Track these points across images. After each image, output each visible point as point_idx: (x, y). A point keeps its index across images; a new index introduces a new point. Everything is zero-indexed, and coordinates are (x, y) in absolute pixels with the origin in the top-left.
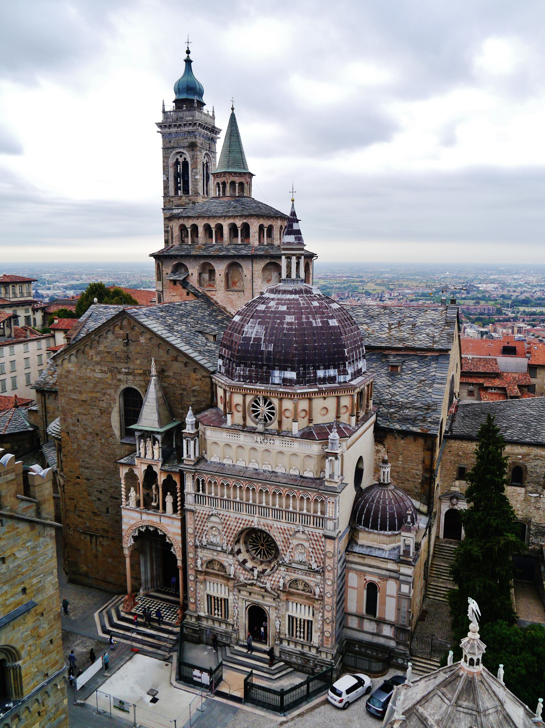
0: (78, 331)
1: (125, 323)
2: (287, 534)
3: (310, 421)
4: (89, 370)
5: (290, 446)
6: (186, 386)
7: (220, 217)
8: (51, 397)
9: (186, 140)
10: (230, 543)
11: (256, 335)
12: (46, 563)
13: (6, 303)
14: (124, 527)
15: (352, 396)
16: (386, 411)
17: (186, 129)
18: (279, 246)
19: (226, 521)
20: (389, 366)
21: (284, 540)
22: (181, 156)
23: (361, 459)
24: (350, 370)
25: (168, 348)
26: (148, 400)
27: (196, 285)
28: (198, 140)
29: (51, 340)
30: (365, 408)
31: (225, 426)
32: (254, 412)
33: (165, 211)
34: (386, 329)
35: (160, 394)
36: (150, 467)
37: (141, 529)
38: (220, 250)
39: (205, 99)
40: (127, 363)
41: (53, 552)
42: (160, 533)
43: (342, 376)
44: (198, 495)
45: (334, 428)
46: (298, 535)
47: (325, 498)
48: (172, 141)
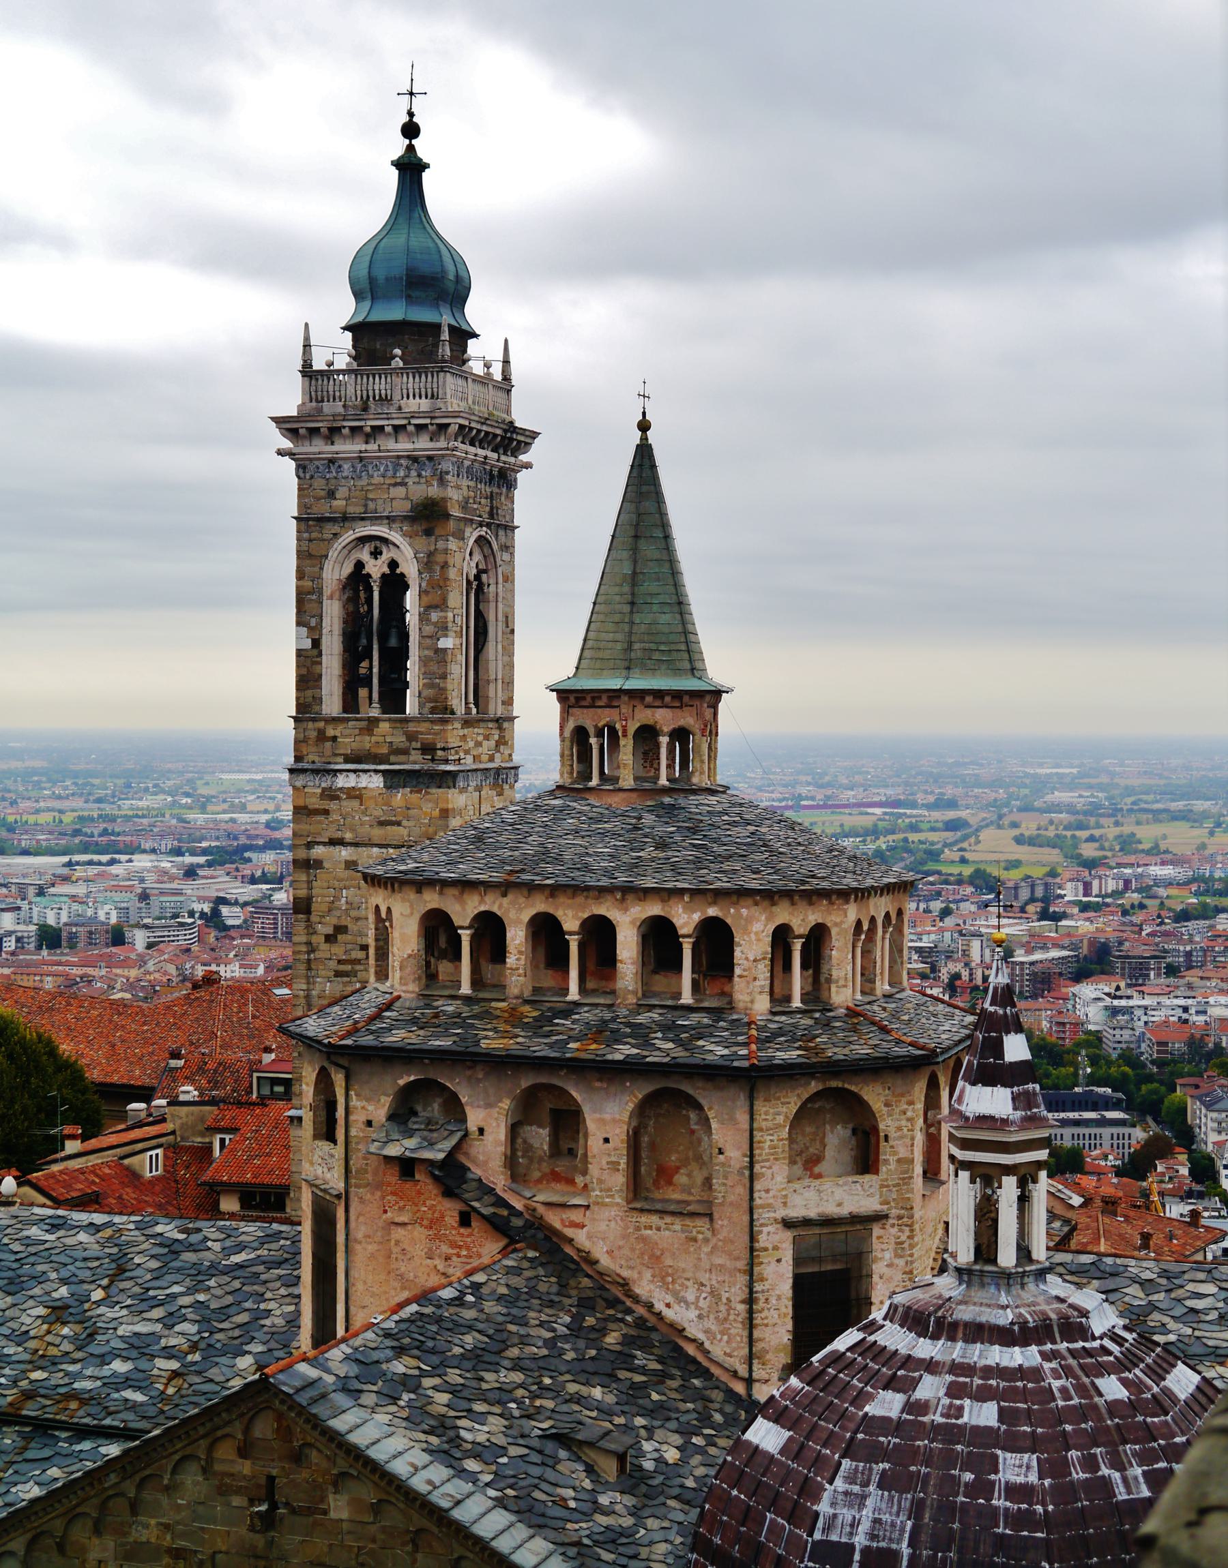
1: (264, 1428)
7: (602, 891)
9: (400, 492)
11: (873, 1537)
17: (403, 445)
18: (852, 1013)
22: (376, 554)
25: (459, 1551)
27: (499, 1181)
33: (300, 781)
38: (603, 1032)
39: (475, 312)
48: (342, 492)
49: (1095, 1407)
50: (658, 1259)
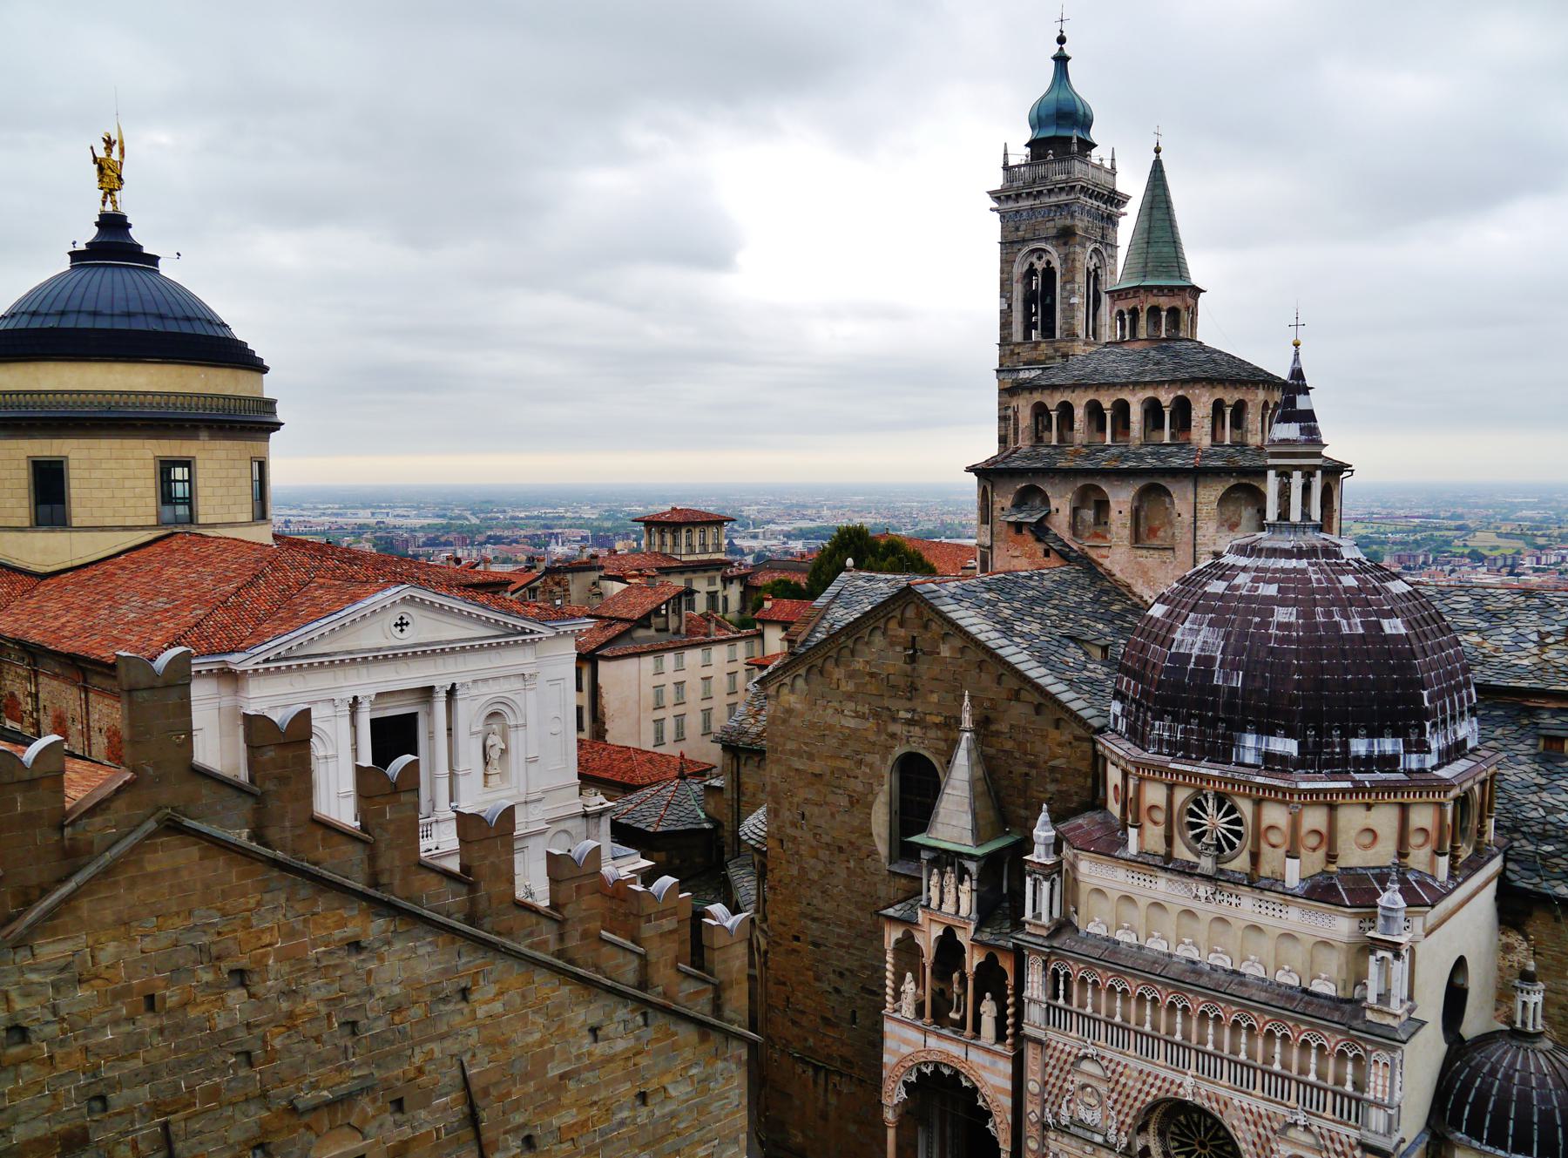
0: (812, 624)
1: (910, 613)
2: (1264, 1127)
3: (1331, 858)
4: (830, 711)
5: (1278, 914)
6: (1036, 756)
7: (1124, 385)
8: (750, 762)
9: (1052, 224)
10: (1125, 1128)
11: (1202, 650)
12: (726, 1116)
13: (674, 564)
14: (886, 1058)
15: (1441, 805)
16: (1531, 848)
17: (1053, 199)
18: (1260, 448)
19: (1116, 1076)
20: (1538, 737)
21: (1256, 1140)
22: (1040, 258)
23: (1460, 964)
24: (1436, 743)
26: (951, 782)
27: (1066, 535)
28: (1077, 222)
29: (757, 642)
30: (1475, 838)
31: (1124, 855)
32: (1193, 826)
34: (1531, 645)
35: (979, 773)
36: (949, 932)
37: (925, 1070)
38: (1122, 457)
39: (1095, 134)
40: (910, 699)
41: (740, 1095)
42: (965, 1084)
43: (1414, 757)
44: (1054, 1007)
45: (1393, 882)
46: (1292, 1133)
47: (1365, 1050)
48: (1022, 227)
49: (1337, 589)
50: (1146, 573)
